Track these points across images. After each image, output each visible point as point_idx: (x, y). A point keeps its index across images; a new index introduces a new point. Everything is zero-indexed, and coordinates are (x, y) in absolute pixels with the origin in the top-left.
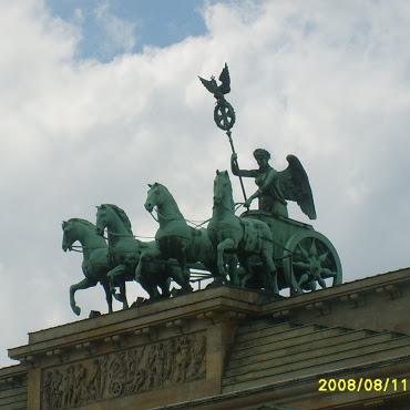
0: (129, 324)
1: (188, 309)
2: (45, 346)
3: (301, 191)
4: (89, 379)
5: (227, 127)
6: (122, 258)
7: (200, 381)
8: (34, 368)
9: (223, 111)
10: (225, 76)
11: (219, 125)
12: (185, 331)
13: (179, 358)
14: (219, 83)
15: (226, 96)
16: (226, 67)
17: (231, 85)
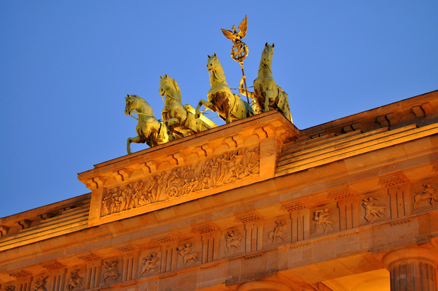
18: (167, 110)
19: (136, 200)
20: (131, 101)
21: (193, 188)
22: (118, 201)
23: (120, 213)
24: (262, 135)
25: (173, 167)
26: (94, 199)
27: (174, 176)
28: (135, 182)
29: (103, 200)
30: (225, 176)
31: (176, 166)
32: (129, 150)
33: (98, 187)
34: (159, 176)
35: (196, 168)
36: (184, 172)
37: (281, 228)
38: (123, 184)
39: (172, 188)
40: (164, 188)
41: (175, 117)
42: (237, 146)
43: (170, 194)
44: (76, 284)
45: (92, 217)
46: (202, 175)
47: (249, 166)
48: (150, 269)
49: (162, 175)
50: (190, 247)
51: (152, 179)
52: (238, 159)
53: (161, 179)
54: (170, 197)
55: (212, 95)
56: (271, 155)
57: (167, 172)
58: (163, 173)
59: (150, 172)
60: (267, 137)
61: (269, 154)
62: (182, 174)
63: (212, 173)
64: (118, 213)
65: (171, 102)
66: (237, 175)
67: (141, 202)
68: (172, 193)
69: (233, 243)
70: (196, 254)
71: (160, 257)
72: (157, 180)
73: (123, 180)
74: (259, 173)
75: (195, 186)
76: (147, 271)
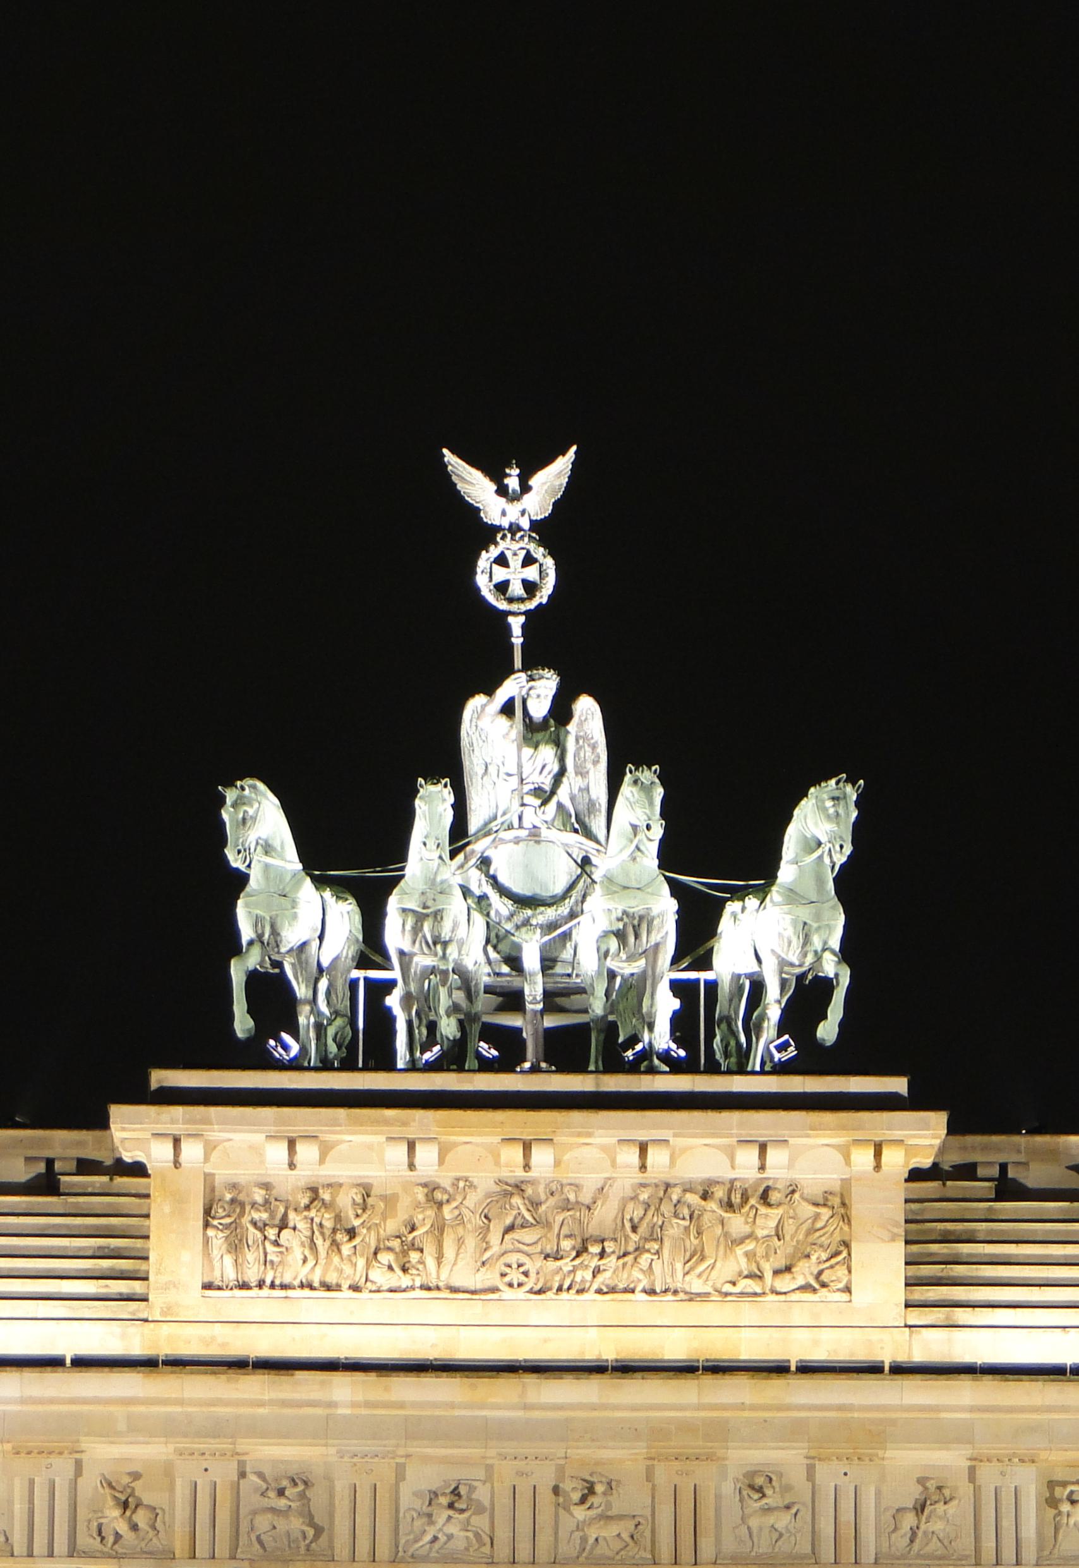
3: (588, 789)
19: (361, 1262)
20: (251, 811)
21: (600, 1278)
22: (276, 1243)
23: (290, 1293)
24: (863, 1158)
25: (505, 1174)
26: (167, 1209)
27: (515, 1212)
28: (341, 1185)
29: (207, 1225)
30: (718, 1264)
31: (520, 1173)
33: (177, 1164)
34: (445, 1191)
35: (599, 1203)
36: (552, 1201)
37: (940, 1508)
38: (290, 1183)
39: (513, 1258)
40: (471, 1242)
42: (762, 1168)
43: (507, 1279)
44: (134, 1527)
45: (163, 1279)
46: (627, 1237)
47: (814, 1258)
48: (450, 1537)
49: (455, 1185)
50: (604, 1494)
51: (421, 1197)
52: (768, 1220)
53: (454, 1204)
55: (625, 912)
56: (893, 1240)
57: (476, 1181)
58: (461, 1184)
59: (412, 1166)
60: (878, 1167)
61: (886, 1235)
62: (543, 1208)
63: (667, 1244)
64: (283, 1293)
65: (439, 879)
66: (768, 1275)
67: (379, 1276)
68: (515, 1276)
69: (771, 1519)
70: (631, 1525)
71: (487, 1503)
72: (440, 1205)
73: (292, 1165)
74: (848, 1290)
75: (608, 1274)
76: (437, 1545)
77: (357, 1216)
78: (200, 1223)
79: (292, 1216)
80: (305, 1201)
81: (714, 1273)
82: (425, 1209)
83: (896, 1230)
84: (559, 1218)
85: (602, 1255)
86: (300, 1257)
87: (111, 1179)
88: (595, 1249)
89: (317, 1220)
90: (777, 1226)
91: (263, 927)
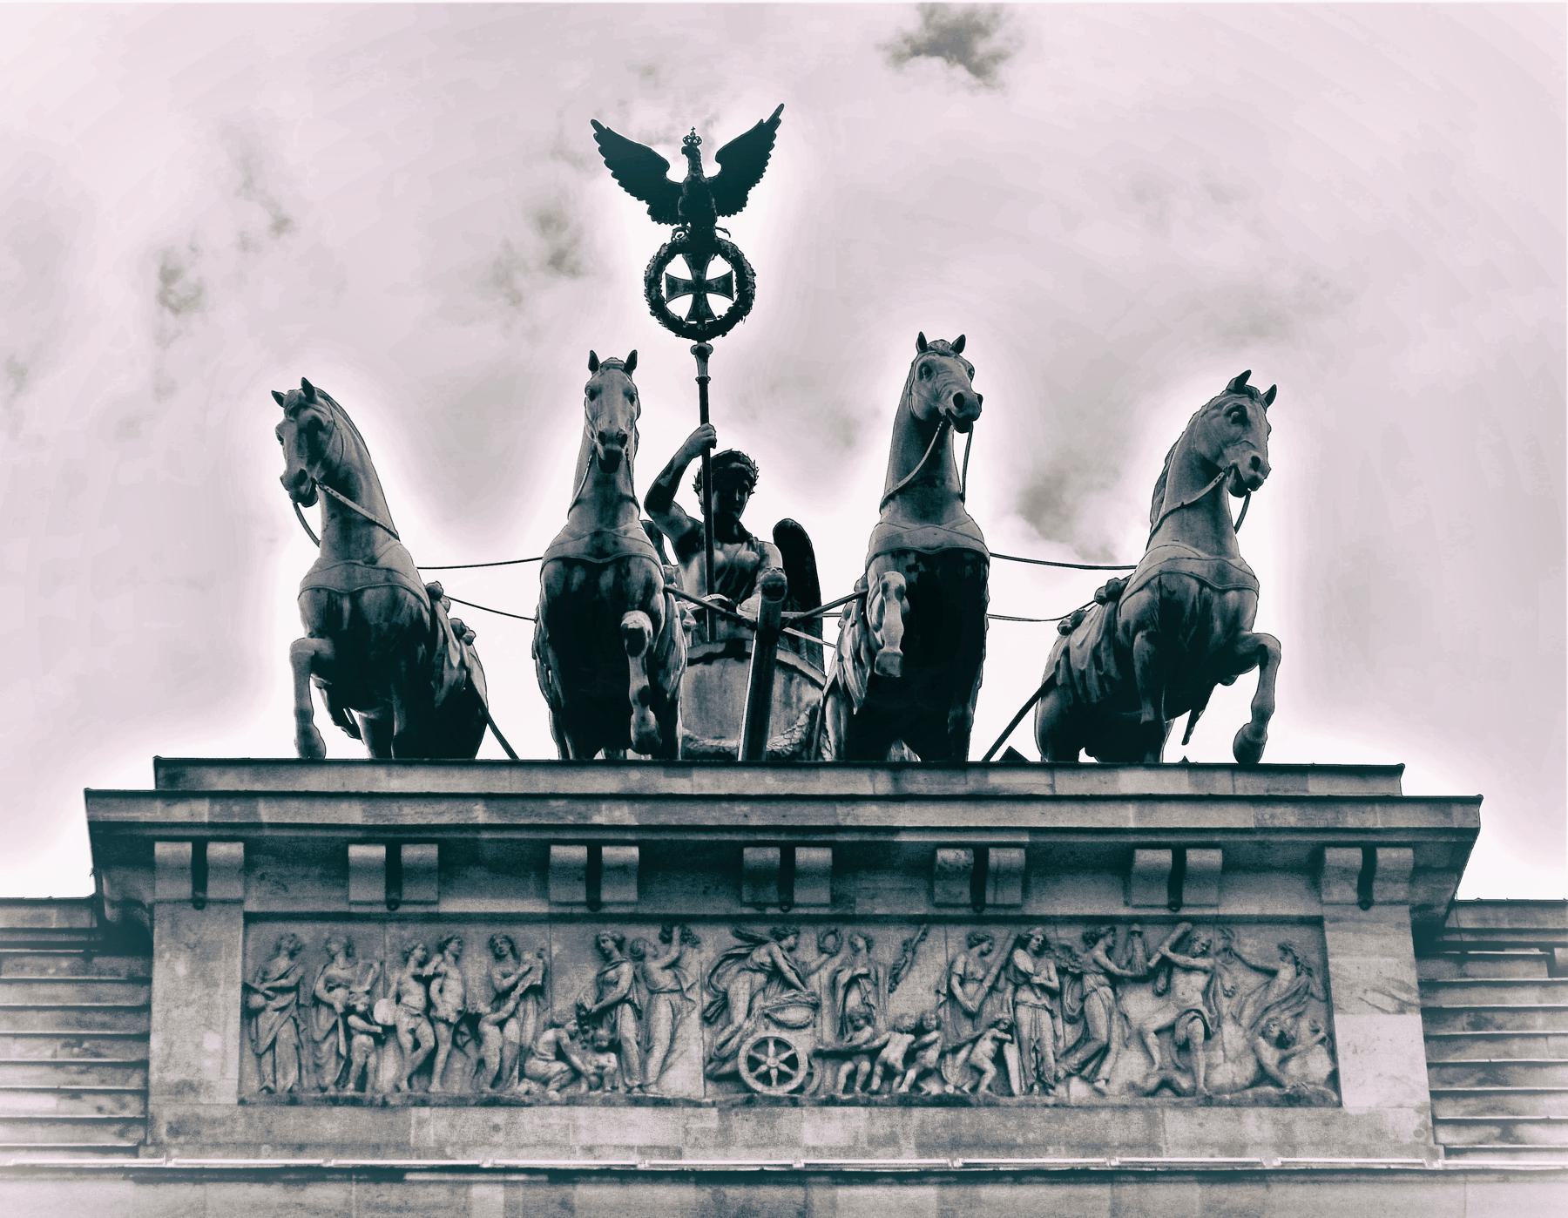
0: (904, 816)
1: (1288, 817)
2: (354, 814)
4: (562, 1005)
5: (701, 330)
6: (650, 587)
7: (1296, 1116)
8: (199, 903)
9: (698, 265)
10: (749, 156)
11: (658, 308)
12: (1196, 902)
13: (1143, 1006)
14: (711, 169)
15: (722, 221)
16: (775, 121)
17: (753, 194)
18: (599, 551)
26: (182, 969)
32: (304, 715)
41: (646, 606)
42: (1176, 903)
45: (173, 1076)
51: (610, 945)
53: (667, 959)
54: (759, 1086)
56: (1401, 1011)
77: (505, 976)
78: (236, 993)
79: (395, 976)
80: (418, 953)
81: (1106, 1068)
82: (617, 965)
83: (1404, 997)
84: (844, 978)
85: (919, 1030)
86: (407, 1040)
87: (87, 957)
88: (908, 1022)
89: (435, 986)
90: (1205, 993)
91: (340, 610)
